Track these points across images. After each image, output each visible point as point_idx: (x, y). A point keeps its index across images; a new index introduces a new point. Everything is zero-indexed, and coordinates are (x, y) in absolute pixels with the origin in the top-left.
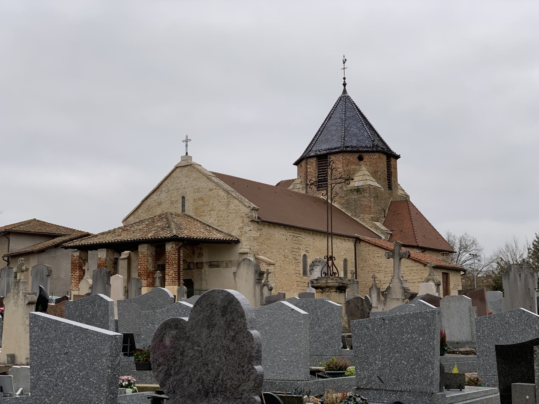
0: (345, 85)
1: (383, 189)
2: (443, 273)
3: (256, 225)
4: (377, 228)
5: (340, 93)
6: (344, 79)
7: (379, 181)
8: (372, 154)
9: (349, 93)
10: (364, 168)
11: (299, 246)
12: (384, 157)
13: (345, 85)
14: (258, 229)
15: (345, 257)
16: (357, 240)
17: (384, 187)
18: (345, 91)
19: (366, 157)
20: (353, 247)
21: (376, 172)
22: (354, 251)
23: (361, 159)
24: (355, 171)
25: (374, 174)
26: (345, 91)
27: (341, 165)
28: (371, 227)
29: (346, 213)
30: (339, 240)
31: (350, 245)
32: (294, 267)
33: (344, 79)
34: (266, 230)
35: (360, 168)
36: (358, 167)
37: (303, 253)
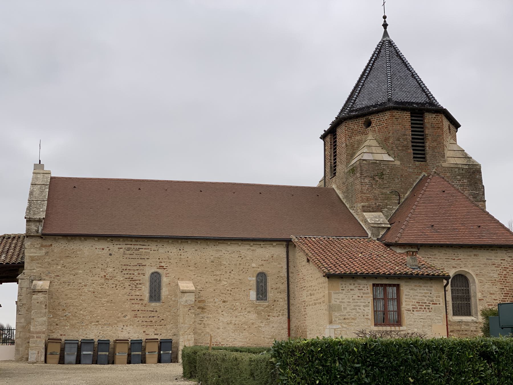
0: (385, 25)
1: (398, 163)
2: (374, 285)
3: (40, 241)
4: (366, 221)
5: (379, 38)
6: (385, 17)
7: (391, 152)
8: (381, 115)
9: (392, 37)
10: (370, 137)
11: (140, 261)
12: (407, 116)
13: (385, 25)
14: (42, 246)
15: (260, 270)
16: (288, 243)
17: (401, 160)
18: (386, 34)
19: (374, 119)
20: (285, 253)
21: (386, 139)
22: (285, 260)
23: (368, 124)
24: (360, 143)
25: (384, 143)
26: (386, 34)
27: (344, 139)
28: (362, 221)
29: (346, 204)
30: (248, 247)
31: (280, 251)
32: (128, 290)
33: (385, 17)
34: (60, 247)
35: (366, 138)
36: (363, 137)
37: (149, 271)
